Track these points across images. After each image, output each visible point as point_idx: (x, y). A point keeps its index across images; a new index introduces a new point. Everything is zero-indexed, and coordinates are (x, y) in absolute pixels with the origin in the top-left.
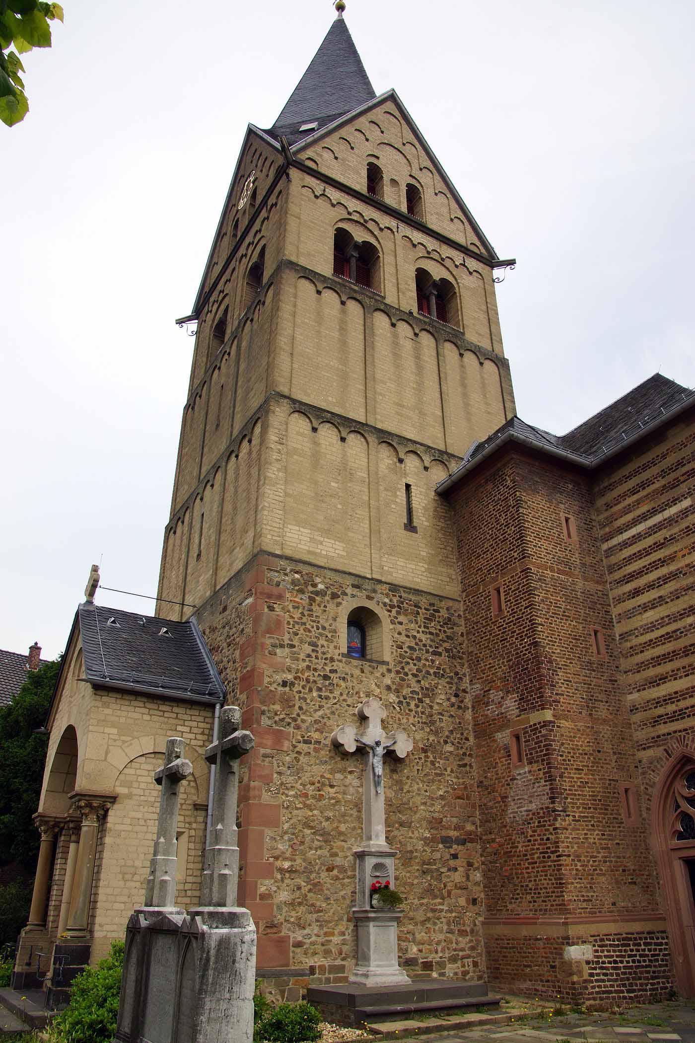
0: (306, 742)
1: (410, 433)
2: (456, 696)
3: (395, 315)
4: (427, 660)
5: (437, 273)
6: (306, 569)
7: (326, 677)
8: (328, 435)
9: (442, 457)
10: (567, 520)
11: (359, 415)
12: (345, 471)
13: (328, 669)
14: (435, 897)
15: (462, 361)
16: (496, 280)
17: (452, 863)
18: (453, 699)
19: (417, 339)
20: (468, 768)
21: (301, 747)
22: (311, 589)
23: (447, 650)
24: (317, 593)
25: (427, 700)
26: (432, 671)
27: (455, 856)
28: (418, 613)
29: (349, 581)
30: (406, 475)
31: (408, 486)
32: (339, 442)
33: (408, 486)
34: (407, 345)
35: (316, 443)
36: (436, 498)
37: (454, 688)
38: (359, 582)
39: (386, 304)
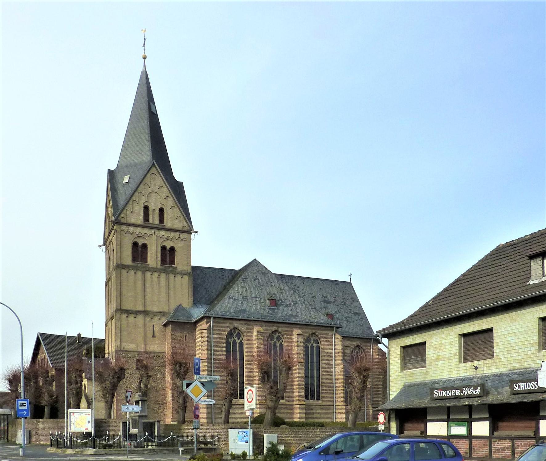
0: (126, 388)
1: (155, 309)
2: (163, 375)
3: (153, 270)
4: (156, 368)
5: (168, 245)
6: (126, 353)
7: (131, 375)
8: (132, 317)
9: (164, 314)
10: (186, 336)
11: (140, 308)
12: (136, 326)
13: (131, 373)
14: (156, 414)
15: (174, 278)
16: (192, 239)
17: (159, 408)
18: (162, 376)
19: (160, 277)
20: (165, 390)
21: (126, 389)
22: (127, 357)
23: (161, 365)
24: (128, 357)
25: (155, 377)
26: (157, 370)
27: (160, 407)
28: (154, 358)
29: (136, 353)
30: (153, 322)
31: (153, 325)
32: (134, 318)
33: (153, 325)
34: (156, 280)
35: (128, 320)
36: (162, 326)
37: (163, 373)
38: (139, 353)
39: (149, 268)
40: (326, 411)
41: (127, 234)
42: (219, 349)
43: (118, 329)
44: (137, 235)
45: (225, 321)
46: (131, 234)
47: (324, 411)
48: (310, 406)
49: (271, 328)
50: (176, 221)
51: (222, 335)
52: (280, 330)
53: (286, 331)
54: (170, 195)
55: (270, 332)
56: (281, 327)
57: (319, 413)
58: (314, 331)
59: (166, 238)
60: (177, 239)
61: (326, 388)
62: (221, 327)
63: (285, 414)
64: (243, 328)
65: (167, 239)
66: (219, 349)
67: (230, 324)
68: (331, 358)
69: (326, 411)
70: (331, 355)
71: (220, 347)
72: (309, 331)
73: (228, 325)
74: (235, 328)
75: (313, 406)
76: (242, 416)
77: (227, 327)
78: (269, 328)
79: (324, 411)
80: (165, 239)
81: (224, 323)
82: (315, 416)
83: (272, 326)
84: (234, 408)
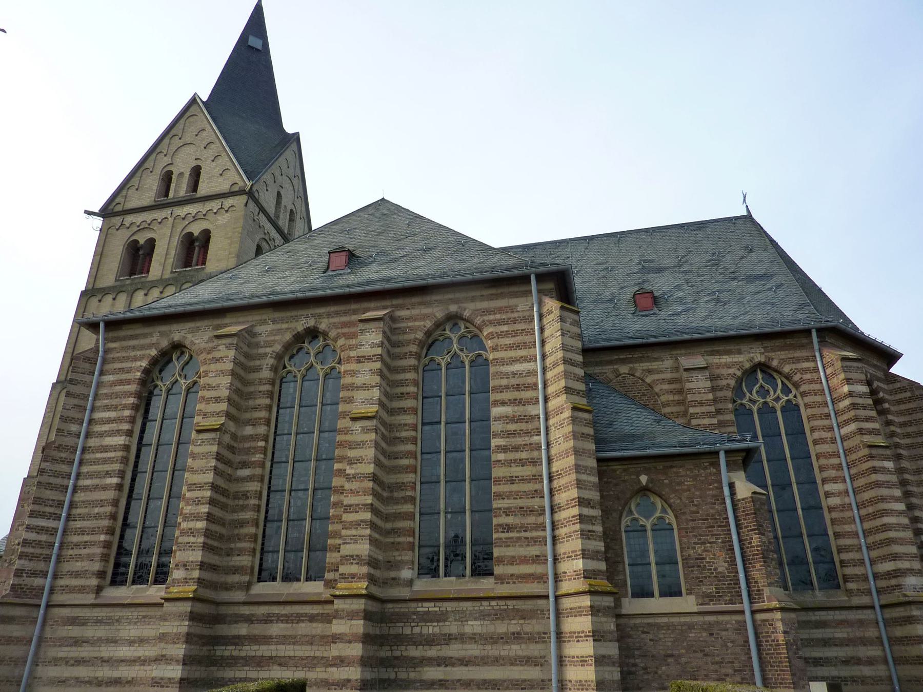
40: (514, 626)
41: (119, 230)
42: (113, 414)
43: (46, 426)
44: (138, 226)
45: (147, 330)
46: (128, 228)
47: (502, 628)
48: (432, 604)
49: (292, 325)
50: (221, 179)
51: (129, 371)
52: (323, 326)
53: (345, 325)
54: (213, 138)
55: (288, 337)
56: (329, 315)
57: (474, 638)
58: (453, 308)
59: (194, 217)
60: (215, 213)
61: (510, 520)
62: (134, 348)
63: (311, 644)
64: (197, 341)
65: (195, 219)
66: (113, 414)
67: (162, 334)
68: (528, 394)
69: (514, 626)
70: (530, 380)
71: (115, 408)
72: (435, 309)
73: (154, 339)
74: (178, 347)
75: (449, 606)
76: (137, 654)
77: (150, 346)
78: (285, 326)
79: (502, 628)
80: (192, 220)
81: (145, 336)
82: (454, 650)
83: (296, 318)
84: (117, 621)
